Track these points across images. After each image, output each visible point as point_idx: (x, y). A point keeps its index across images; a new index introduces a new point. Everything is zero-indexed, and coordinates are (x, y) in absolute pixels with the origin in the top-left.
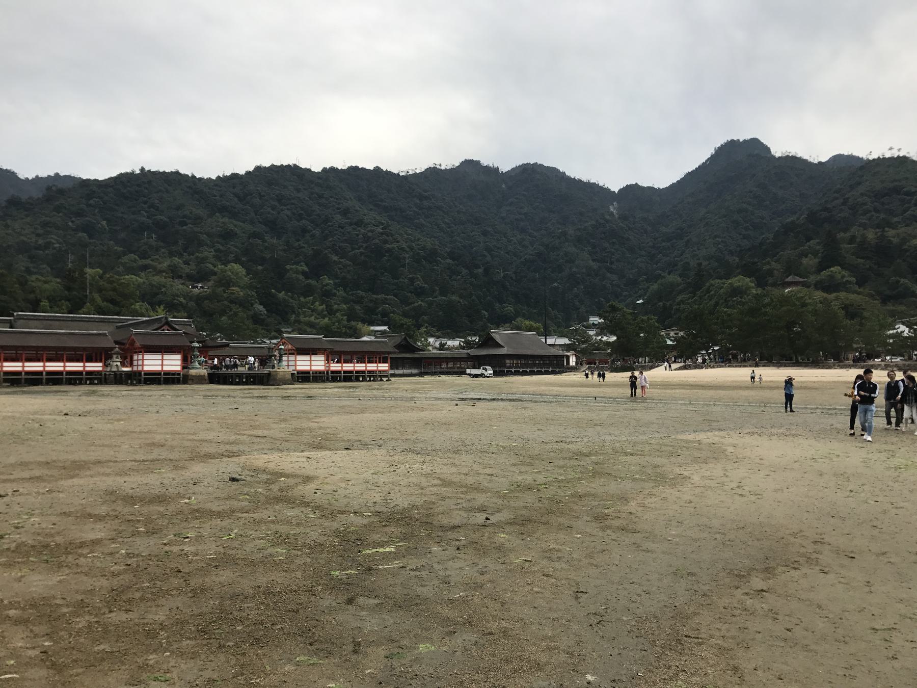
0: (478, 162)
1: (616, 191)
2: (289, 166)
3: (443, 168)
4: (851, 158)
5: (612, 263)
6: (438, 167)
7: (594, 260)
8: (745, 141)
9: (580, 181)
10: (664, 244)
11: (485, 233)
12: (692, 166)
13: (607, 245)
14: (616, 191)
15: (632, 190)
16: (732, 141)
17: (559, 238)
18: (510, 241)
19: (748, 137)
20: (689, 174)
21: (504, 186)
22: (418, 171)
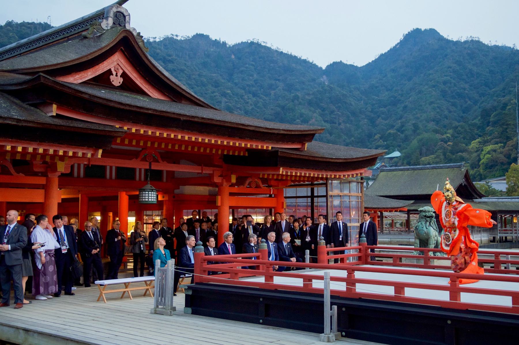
0: (207, 37)
1: (324, 68)
2: (40, 24)
3: (179, 38)
4: (504, 49)
5: (340, 124)
6: (175, 37)
7: (326, 121)
8: (426, 30)
9: (295, 57)
10: (381, 109)
11: (224, 95)
12: (385, 49)
13: (333, 107)
14: (324, 68)
15: (337, 67)
16: (417, 29)
17: (293, 101)
18: (247, 103)
19: (428, 27)
20: (382, 55)
21: (233, 57)
22: (157, 40)
